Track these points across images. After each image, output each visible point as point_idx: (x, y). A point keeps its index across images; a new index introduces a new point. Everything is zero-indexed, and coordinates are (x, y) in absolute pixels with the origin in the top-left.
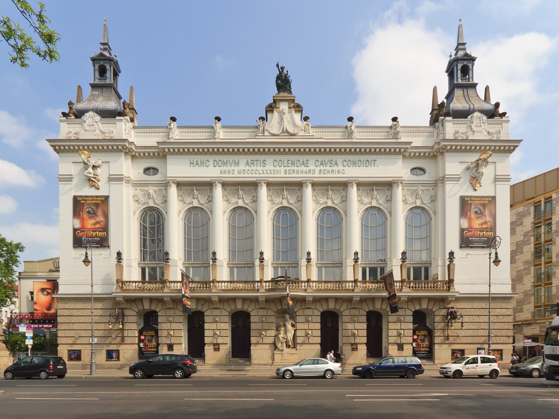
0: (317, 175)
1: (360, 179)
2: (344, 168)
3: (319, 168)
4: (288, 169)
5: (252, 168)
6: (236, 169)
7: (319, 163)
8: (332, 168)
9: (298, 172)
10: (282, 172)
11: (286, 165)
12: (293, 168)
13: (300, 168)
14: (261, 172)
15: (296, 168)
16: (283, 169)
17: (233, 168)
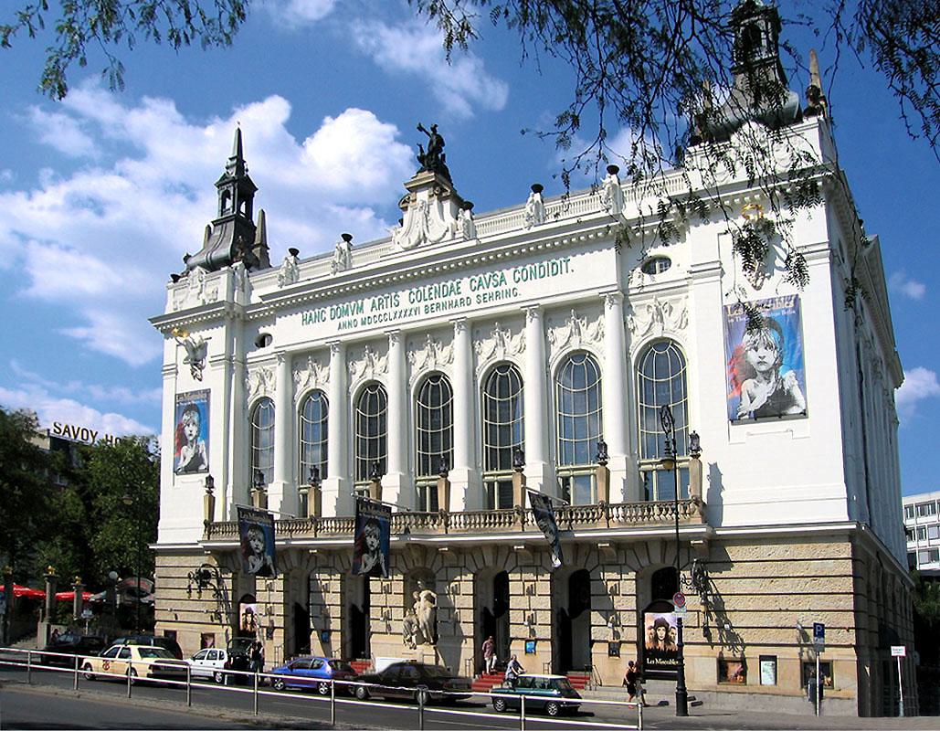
0: (474, 305)
1: (542, 302)
2: (516, 285)
3: (477, 292)
4: (429, 303)
5: (382, 312)
6: (359, 317)
7: (476, 285)
8: (496, 289)
9: (444, 306)
10: (422, 309)
11: (427, 296)
12: (438, 300)
13: (447, 299)
14: (392, 317)
15: (441, 300)
16: (423, 304)
17: (355, 316)
